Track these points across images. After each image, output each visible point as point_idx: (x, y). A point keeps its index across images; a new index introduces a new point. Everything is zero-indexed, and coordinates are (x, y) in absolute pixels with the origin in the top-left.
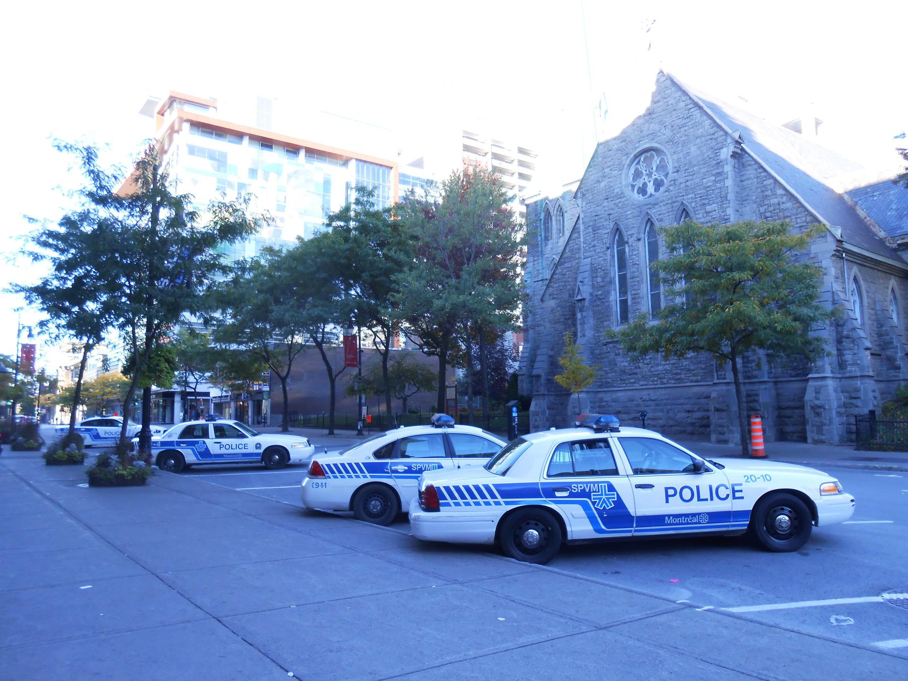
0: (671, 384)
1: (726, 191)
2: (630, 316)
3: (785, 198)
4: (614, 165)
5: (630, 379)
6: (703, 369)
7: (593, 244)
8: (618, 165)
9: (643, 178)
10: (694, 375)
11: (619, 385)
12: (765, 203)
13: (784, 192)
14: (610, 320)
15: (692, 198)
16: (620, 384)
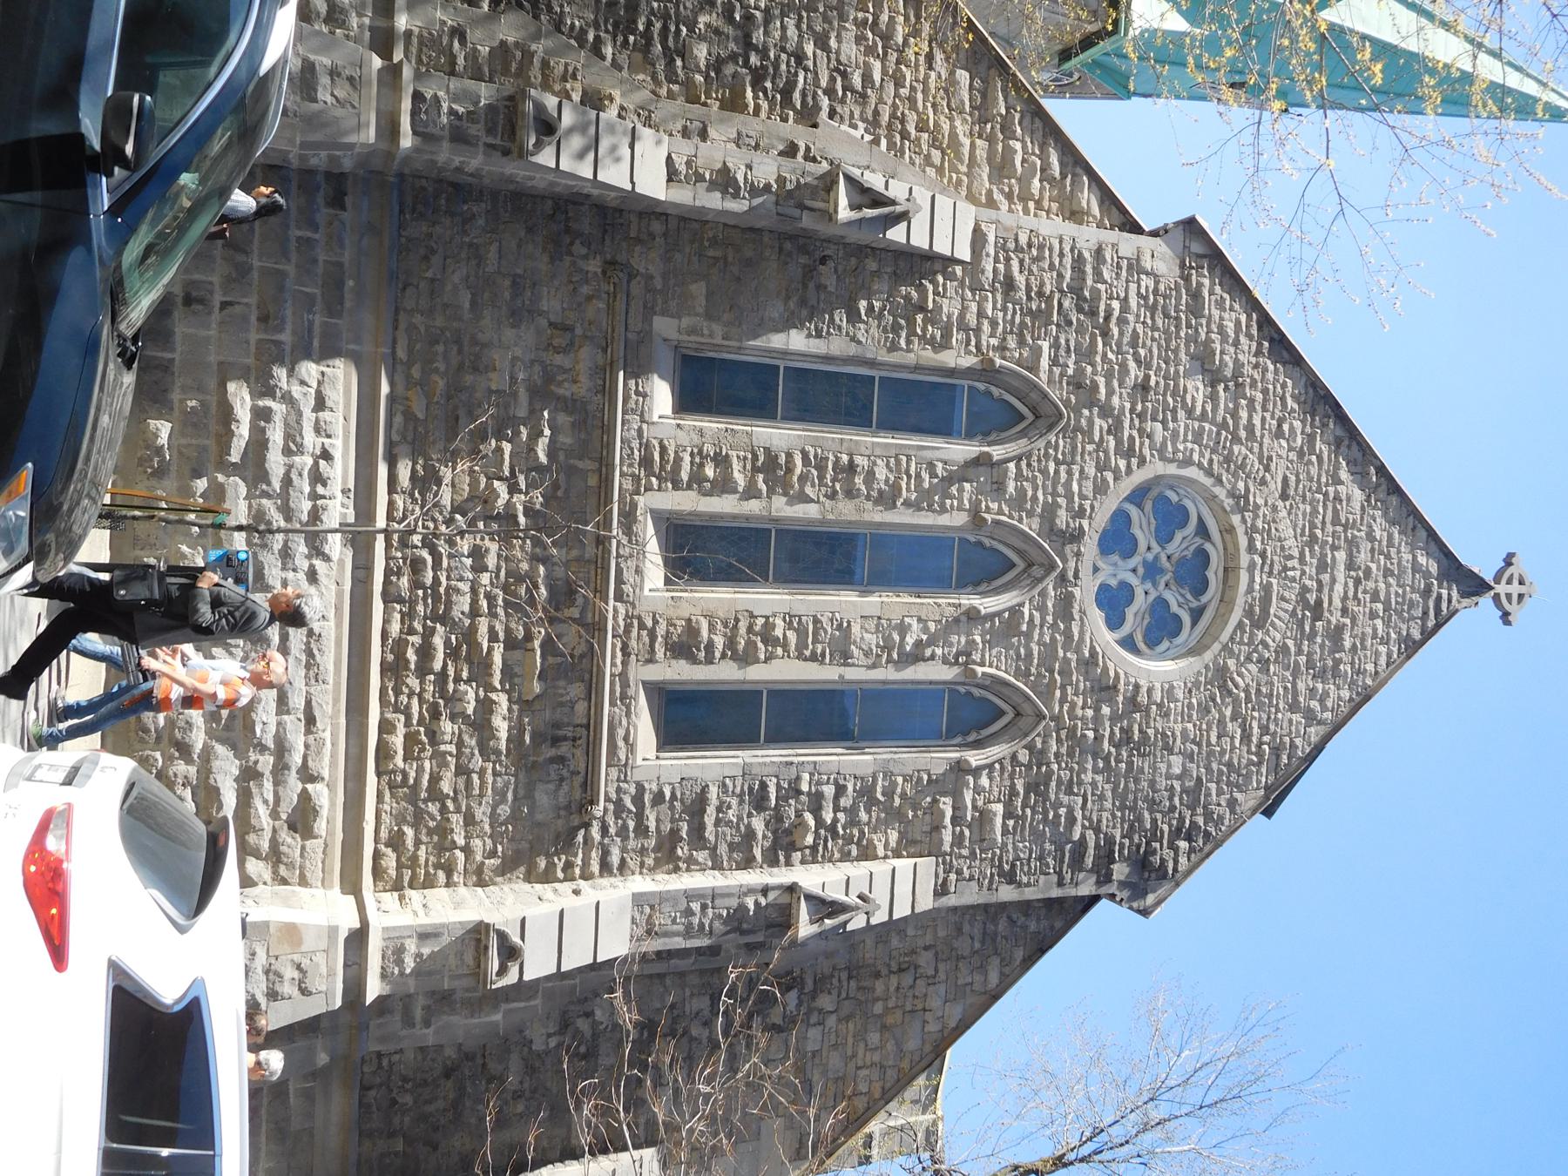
0: (386, 621)
1: (1025, 879)
2: (712, 425)
3: (933, 1027)
4: (1236, 439)
5: (429, 396)
6: (435, 779)
7: (1020, 280)
8: (1231, 451)
9: (1154, 544)
10: (411, 739)
11: (402, 326)
12: (941, 966)
13: (953, 1024)
14: (709, 316)
15: (1043, 752)
16: (411, 328)
